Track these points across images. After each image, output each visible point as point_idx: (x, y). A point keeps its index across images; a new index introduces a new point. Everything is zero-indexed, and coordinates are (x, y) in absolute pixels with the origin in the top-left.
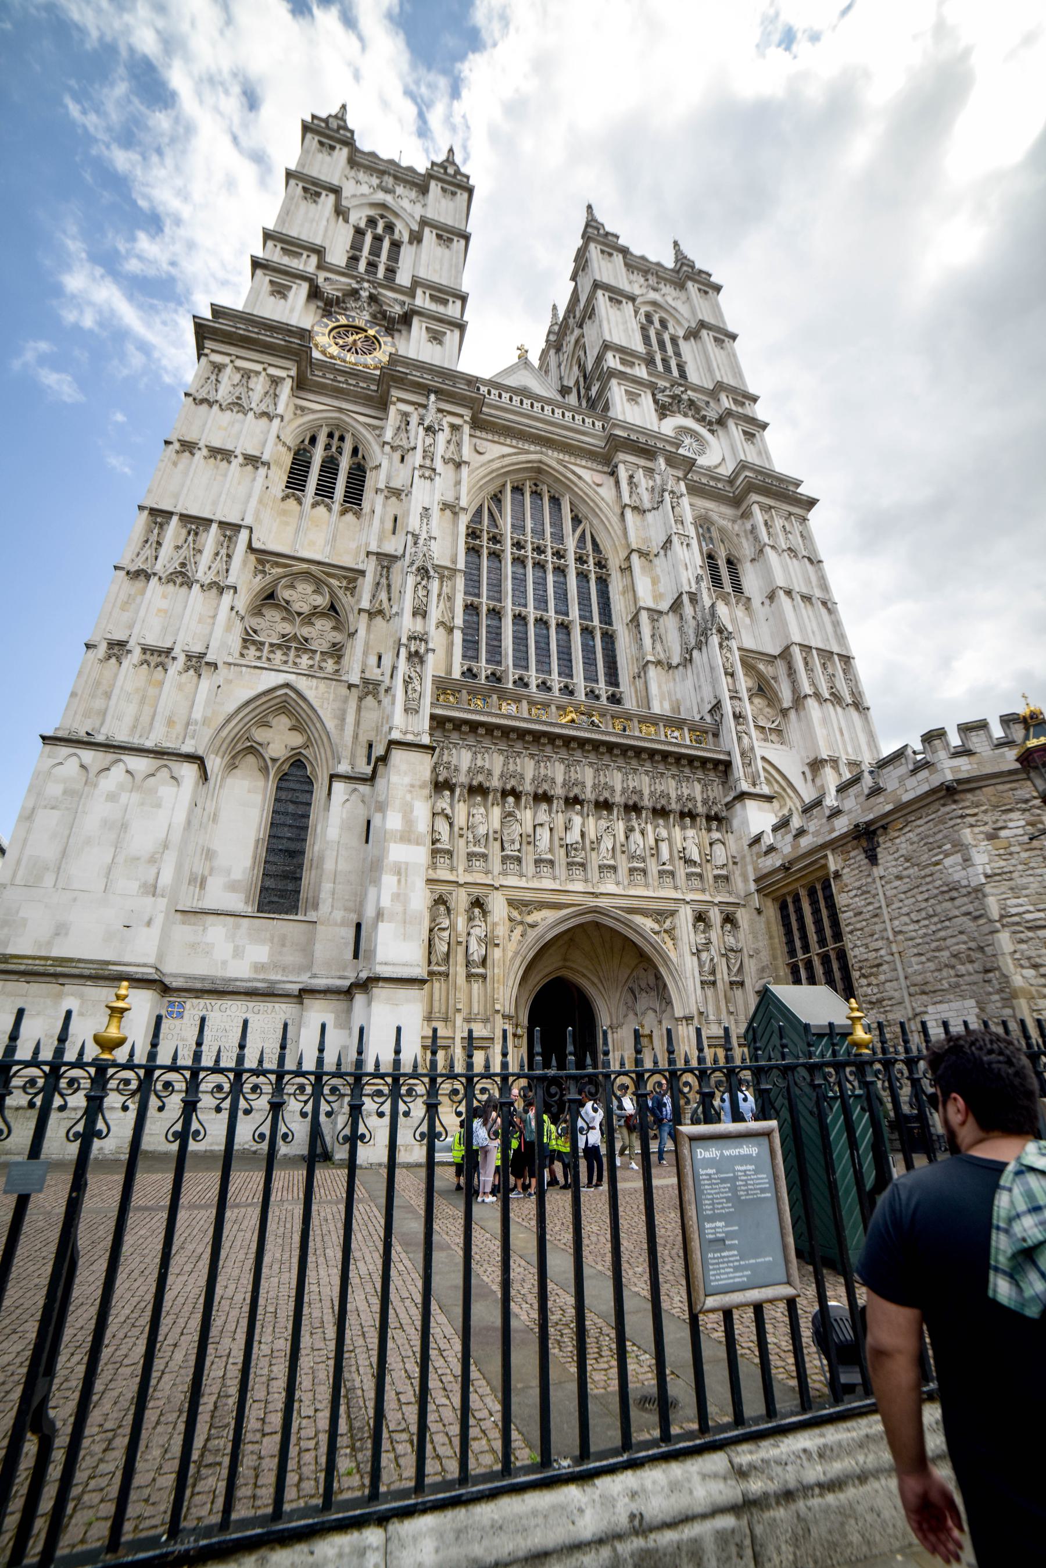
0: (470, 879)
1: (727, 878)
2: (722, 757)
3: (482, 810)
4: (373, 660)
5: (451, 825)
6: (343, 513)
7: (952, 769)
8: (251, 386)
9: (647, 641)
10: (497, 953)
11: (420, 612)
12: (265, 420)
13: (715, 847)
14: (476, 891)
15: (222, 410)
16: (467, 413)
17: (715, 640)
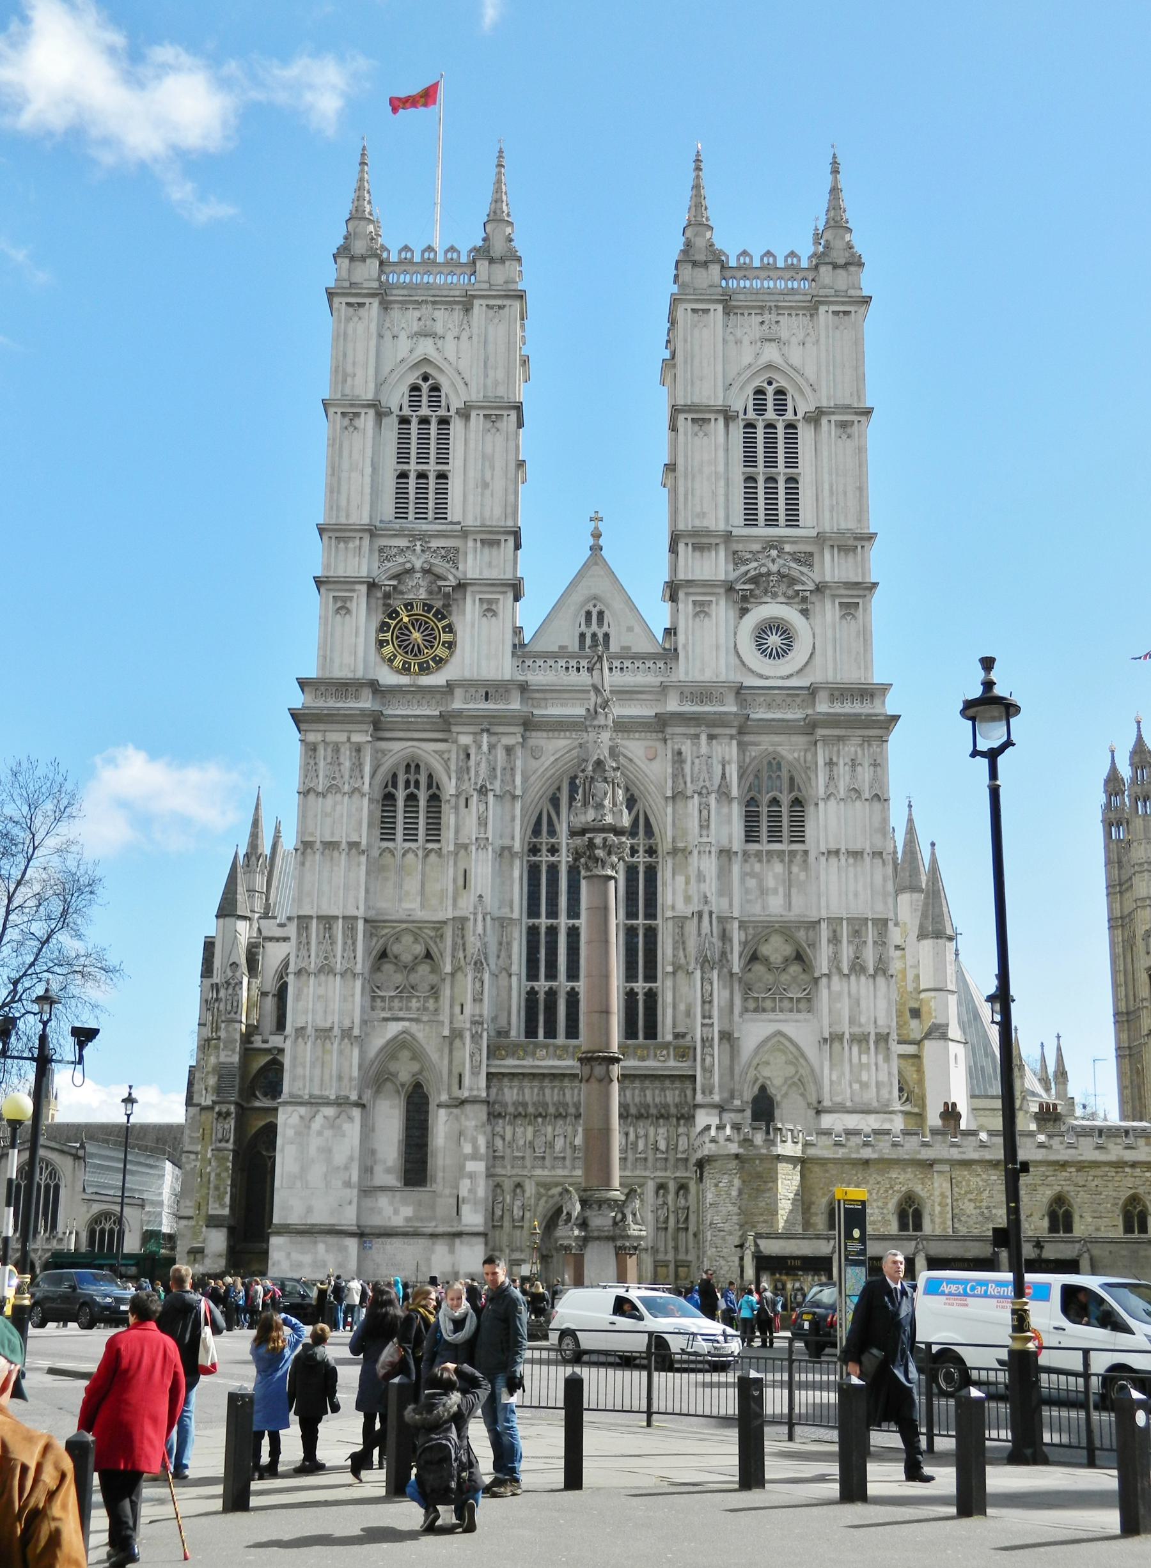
0: (514, 1173)
1: (686, 1160)
2: (690, 1073)
3: (522, 1129)
4: (457, 1009)
5: (504, 1139)
6: (428, 853)
7: (710, 1149)
8: (342, 760)
10: (528, 1215)
11: (477, 999)
12: (356, 795)
13: (680, 1139)
14: (518, 1179)
15: (324, 796)
16: (520, 729)
17: (698, 974)
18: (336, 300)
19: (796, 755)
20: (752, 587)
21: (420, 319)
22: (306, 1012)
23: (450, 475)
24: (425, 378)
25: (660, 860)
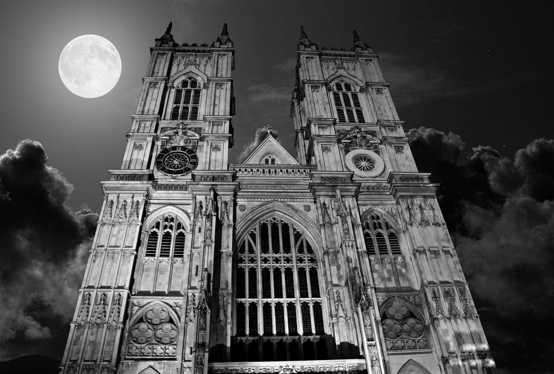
9: (333, 309)
15: (113, 226)
18: (154, 52)
19: (387, 210)
20: (350, 141)
21: (189, 61)
22: (78, 353)
23: (199, 107)
24: (190, 79)
25: (319, 264)
